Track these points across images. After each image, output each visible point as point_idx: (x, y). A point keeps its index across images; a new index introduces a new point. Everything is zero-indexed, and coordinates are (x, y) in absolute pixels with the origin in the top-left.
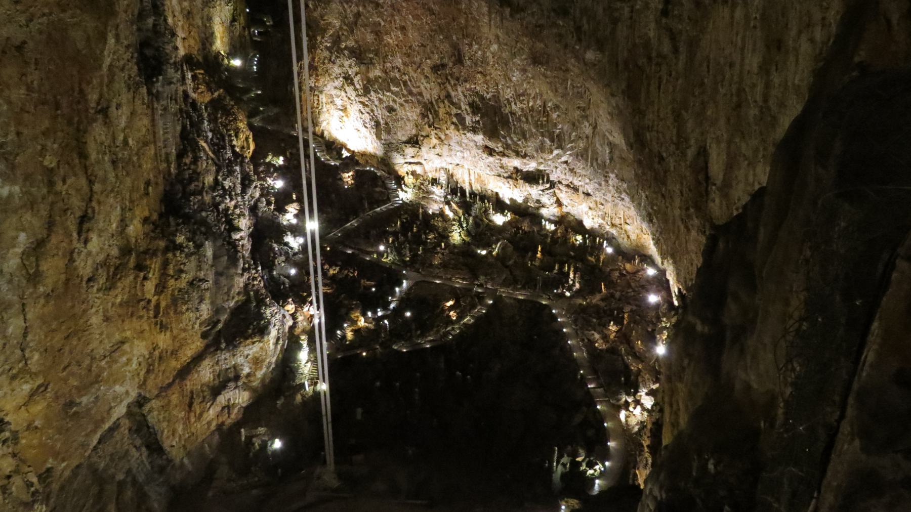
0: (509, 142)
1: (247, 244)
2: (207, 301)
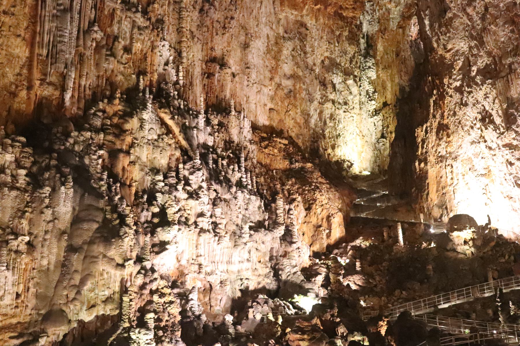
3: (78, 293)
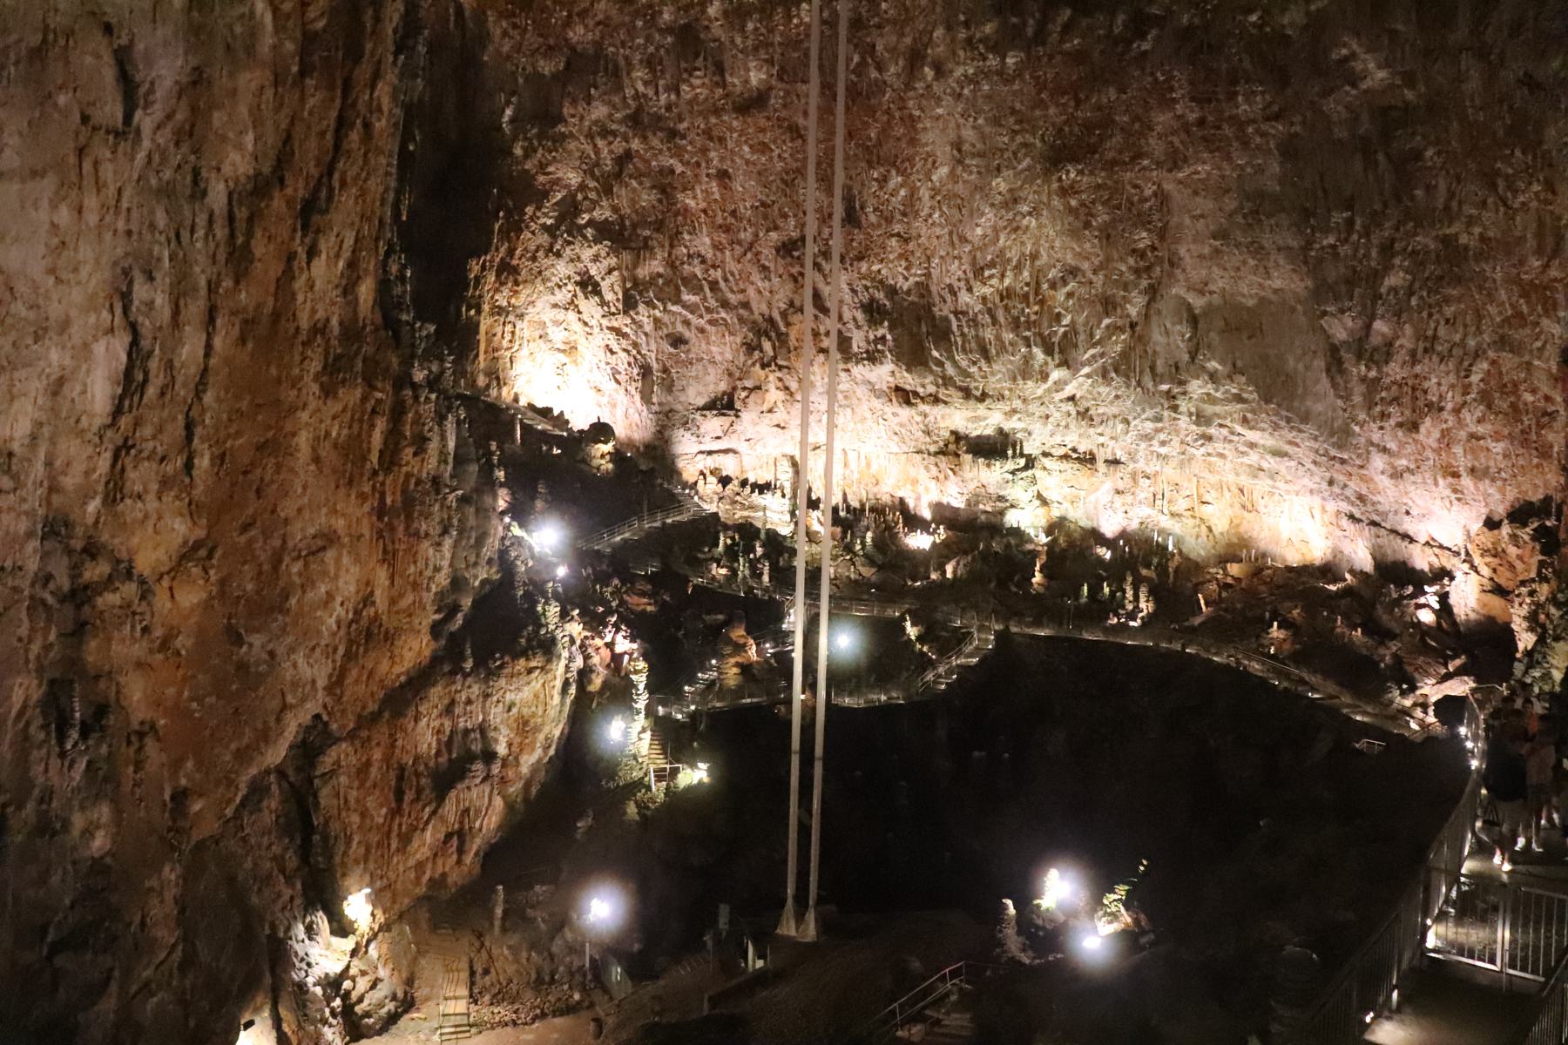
0: (950, 370)
3: (478, 556)
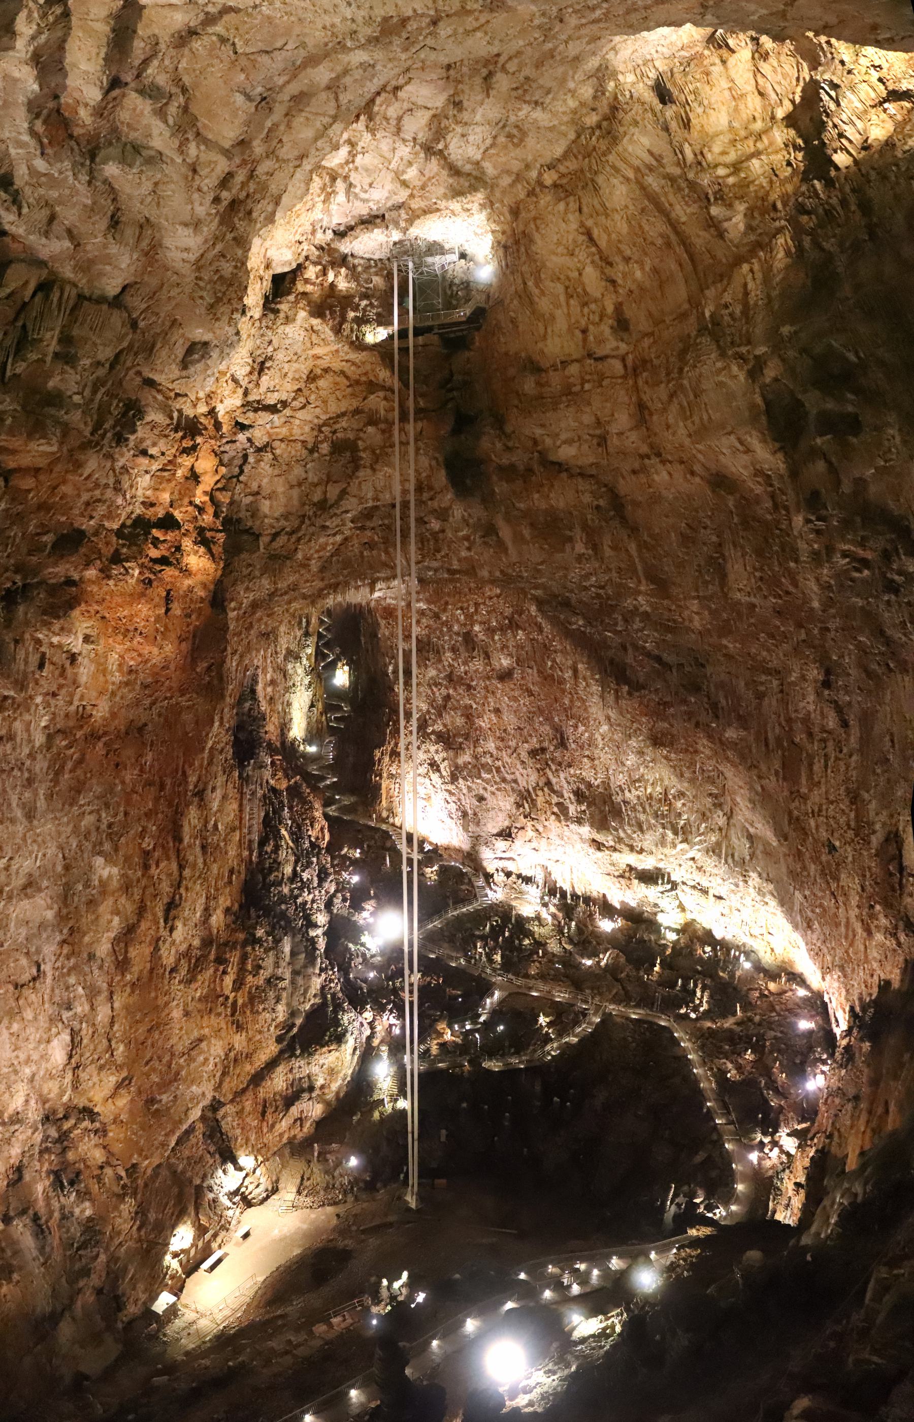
1: (322, 944)
2: (284, 1001)
